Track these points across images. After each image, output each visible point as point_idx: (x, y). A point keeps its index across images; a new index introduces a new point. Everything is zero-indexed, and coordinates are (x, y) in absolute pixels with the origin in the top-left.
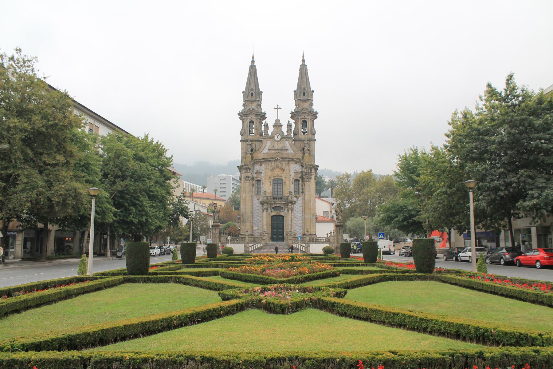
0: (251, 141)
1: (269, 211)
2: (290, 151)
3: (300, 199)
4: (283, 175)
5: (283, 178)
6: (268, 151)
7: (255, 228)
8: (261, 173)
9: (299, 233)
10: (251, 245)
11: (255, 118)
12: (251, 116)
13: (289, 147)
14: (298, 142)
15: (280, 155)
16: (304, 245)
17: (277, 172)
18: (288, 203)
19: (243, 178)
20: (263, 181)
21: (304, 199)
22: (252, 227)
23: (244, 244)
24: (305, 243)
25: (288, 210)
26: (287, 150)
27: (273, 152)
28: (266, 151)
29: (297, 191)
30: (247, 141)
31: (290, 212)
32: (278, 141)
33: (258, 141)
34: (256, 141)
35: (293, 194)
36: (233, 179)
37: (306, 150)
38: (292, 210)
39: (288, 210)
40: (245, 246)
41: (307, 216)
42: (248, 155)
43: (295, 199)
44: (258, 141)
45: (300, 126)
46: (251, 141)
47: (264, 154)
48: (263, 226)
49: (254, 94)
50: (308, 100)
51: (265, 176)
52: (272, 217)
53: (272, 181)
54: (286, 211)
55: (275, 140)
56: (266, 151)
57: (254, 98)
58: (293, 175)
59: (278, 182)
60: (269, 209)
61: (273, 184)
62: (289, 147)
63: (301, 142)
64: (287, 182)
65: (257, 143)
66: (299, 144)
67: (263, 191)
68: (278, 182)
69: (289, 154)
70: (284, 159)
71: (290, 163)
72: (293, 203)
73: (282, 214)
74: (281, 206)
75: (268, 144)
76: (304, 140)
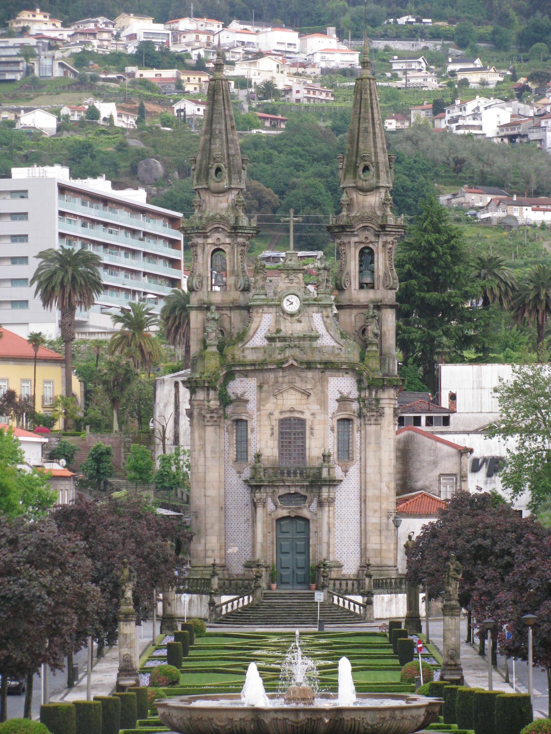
0: (218, 308)
1: (271, 506)
2: (327, 341)
3: (354, 470)
4: (308, 410)
5: (307, 416)
6: (265, 343)
7: (233, 550)
8: (247, 401)
9: (351, 567)
10: (225, 598)
11: (228, 240)
12: (217, 235)
13: (321, 328)
14: (348, 311)
15: (296, 352)
16: (359, 599)
17: (291, 400)
18: (320, 487)
19: (195, 413)
20: (252, 424)
21: (363, 471)
22: (224, 547)
23: (206, 598)
24: (363, 595)
25: (321, 504)
26: (316, 338)
27: (279, 344)
28: (258, 340)
29: (345, 451)
30: (208, 309)
31: (326, 509)
32: (292, 315)
33: (239, 307)
34: (231, 309)
35: (334, 457)
36: (63, 189)
37: (370, 335)
38: (331, 501)
39: (321, 504)
40: (212, 604)
41: (373, 520)
42: (209, 349)
43: (338, 473)
44: (239, 307)
45: (353, 265)
46: (218, 308)
47: (254, 349)
48: (254, 546)
49: (225, 171)
50: (378, 188)
51: (259, 410)
52: (279, 520)
53: (276, 423)
54: (314, 505)
55: (284, 312)
56: (258, 340)
57: (225, 184)
58: (333, 406)
59: (292, 431)
60: (269, 500)
61: (281, 433)
62: (321, 328)
63: (355, 312)
64: (318, 429)
65: (236, 317)
66: (351, 319)
67: (252, 451)
68: (292, 431)
69: (319, 350)
70: (309, 366)
71: (327, 373)
72: (333, 483)
73: (305, 513)
74: (303, 492)
75: (264, 323)
76: (366, 307)
